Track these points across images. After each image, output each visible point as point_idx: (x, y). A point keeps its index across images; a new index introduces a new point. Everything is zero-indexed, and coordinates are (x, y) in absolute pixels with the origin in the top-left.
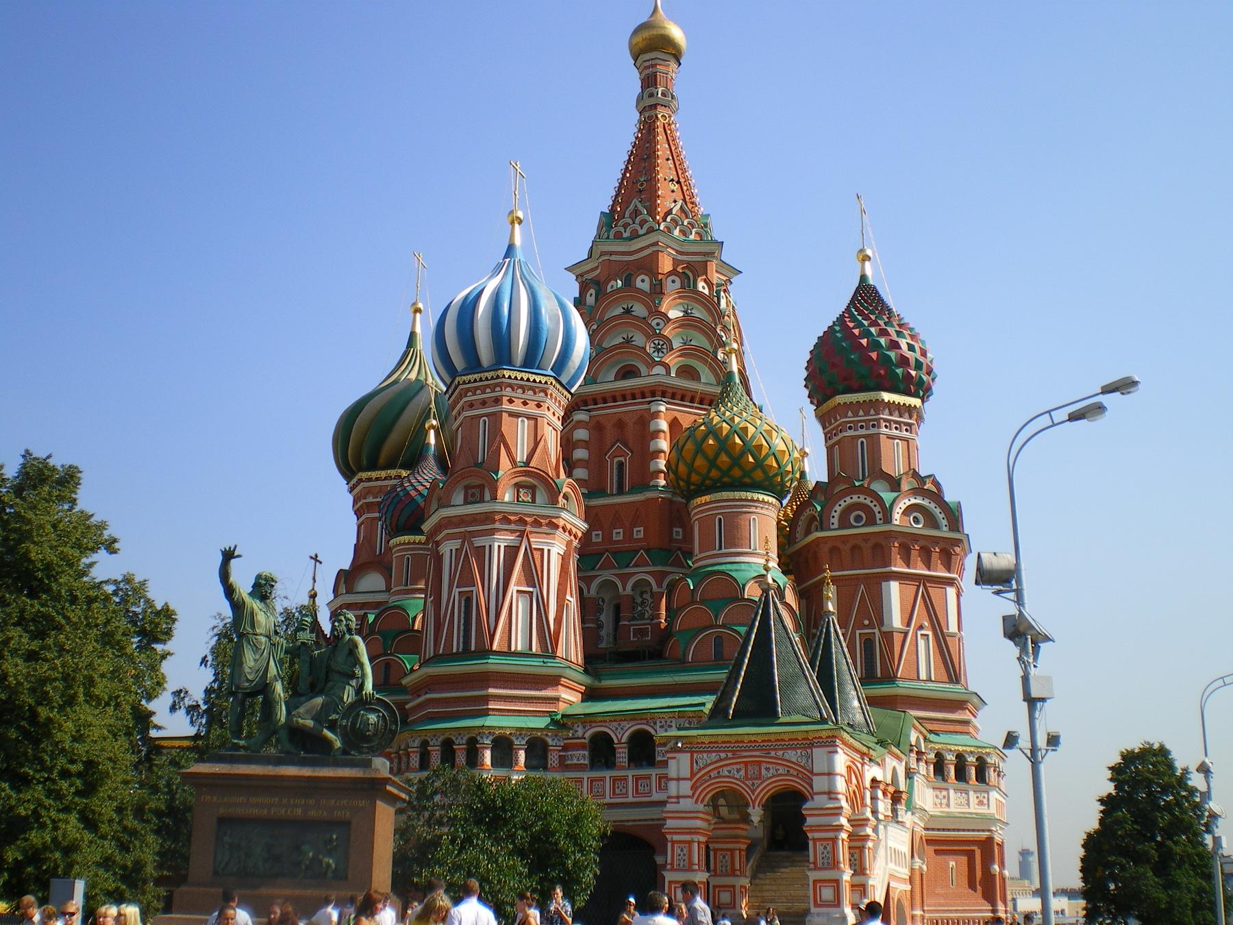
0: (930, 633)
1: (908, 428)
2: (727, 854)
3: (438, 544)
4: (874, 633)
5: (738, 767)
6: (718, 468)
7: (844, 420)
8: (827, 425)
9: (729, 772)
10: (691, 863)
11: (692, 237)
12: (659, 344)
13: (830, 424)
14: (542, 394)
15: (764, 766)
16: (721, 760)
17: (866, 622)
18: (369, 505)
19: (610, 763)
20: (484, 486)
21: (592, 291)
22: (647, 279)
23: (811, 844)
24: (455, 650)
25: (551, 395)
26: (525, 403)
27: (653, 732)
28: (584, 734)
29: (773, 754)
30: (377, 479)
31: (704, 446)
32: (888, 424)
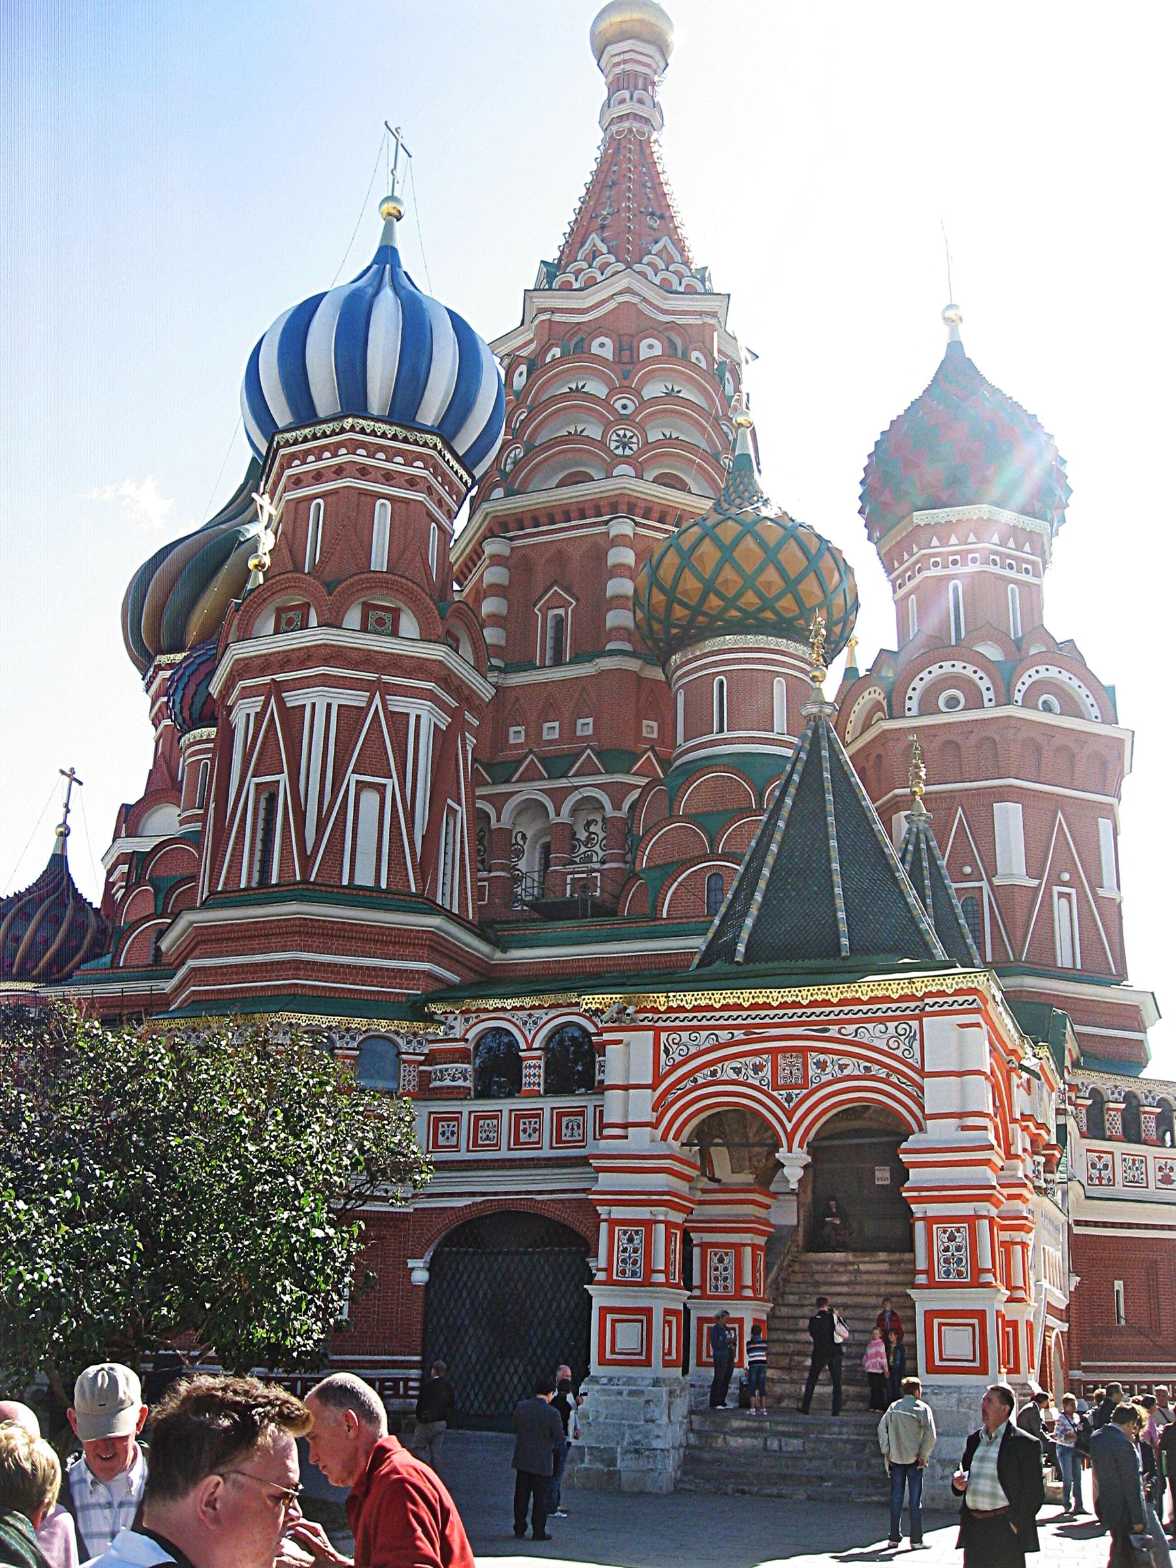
1: (1029, 567)
2: (727, 1254)
3: (230, 709)
4: (981, 888)
5: (757, 1060)
7: (923, 552)
8: (896, 565)
9: (737, 1071)
10: (650, 1271)
11: (681, 289)
12: (625, 436)
13: (901, 563)
14: (419, 464)
15: (813, 1057)
19: (514, 1088)
20: (307, 606)
21: (523, 368)
22: (608, 341)
23: (919, 1227)
24: (243, 886)
25: (436, 466)
26: (389, 477)
28: (467, 1031)
29: (833, 1031)
31: (696, 554)
32: (997, 558)
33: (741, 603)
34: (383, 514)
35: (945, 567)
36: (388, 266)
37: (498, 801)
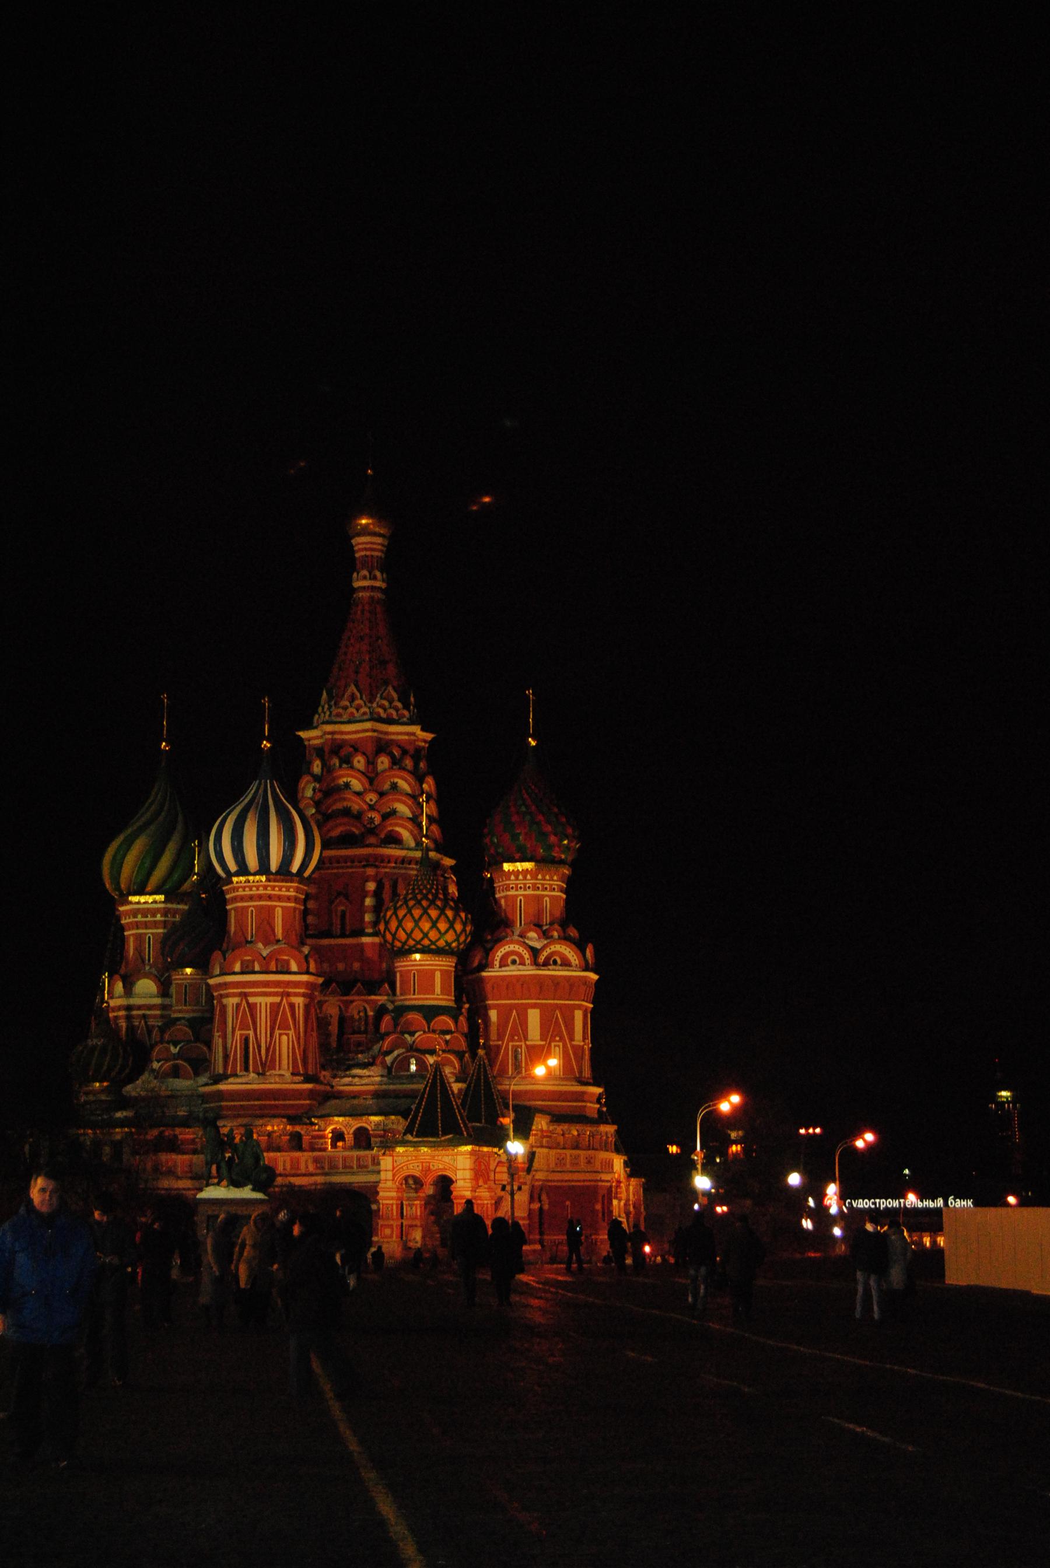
0: (561, 1044)
1: (556, 887)
5: (418, 1164)
6: (414, 940)
7: (507, 882)
8: (497, 881)
9: (413, 1166)
13: (499, 882)
14: (292, 890)
15: (431, 1164)
16: (408, 1161)
17: (516, 1038)
18: (137, 922)
20: (254, 961)
23: (455, 1205)
26: (279, 898)
27: (370, 1128)
29: (436, 1158)
30: (146, 903)
33: (422, 943)
34: (279, 912)
35: (517, 890)
36: (268, 781)
37: (321, 1004)
